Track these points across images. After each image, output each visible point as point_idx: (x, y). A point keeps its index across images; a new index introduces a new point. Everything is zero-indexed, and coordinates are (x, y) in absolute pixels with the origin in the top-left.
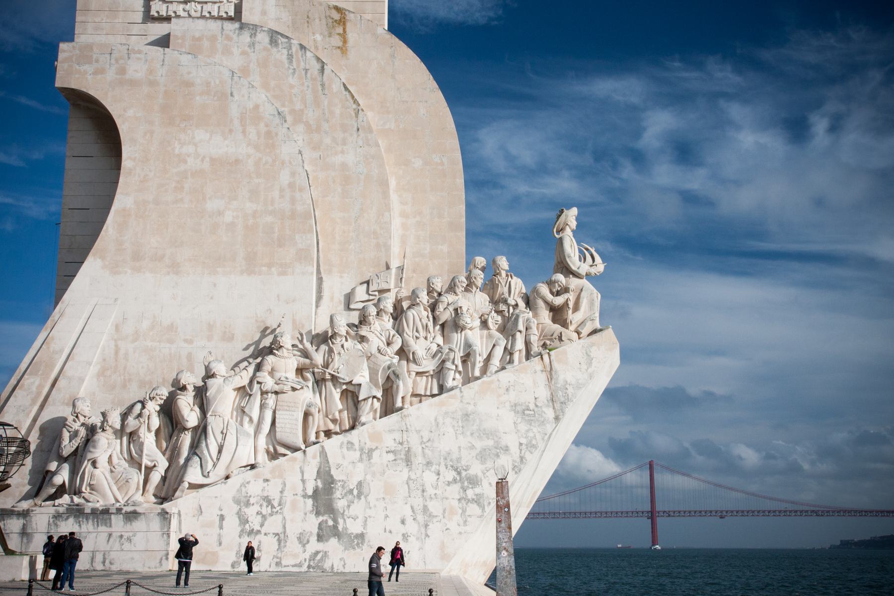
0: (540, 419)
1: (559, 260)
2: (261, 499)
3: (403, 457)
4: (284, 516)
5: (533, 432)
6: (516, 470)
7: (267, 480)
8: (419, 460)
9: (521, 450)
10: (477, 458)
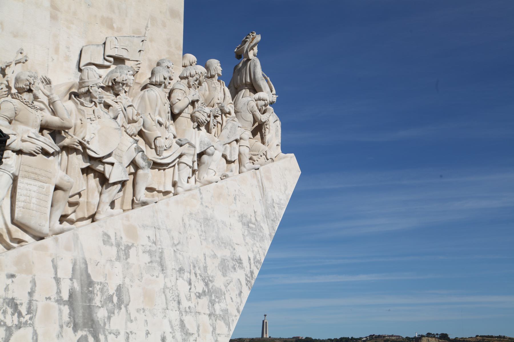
0: (260, 234)
1: (249, 80)
2: (4, 302)
3: (158, 259)
4: (35, 328)
5: (257, 247)
6: (249, 285)
7: (13, 276)
8: (170, 264)
9: (250, 265)
10: (220, 270)
